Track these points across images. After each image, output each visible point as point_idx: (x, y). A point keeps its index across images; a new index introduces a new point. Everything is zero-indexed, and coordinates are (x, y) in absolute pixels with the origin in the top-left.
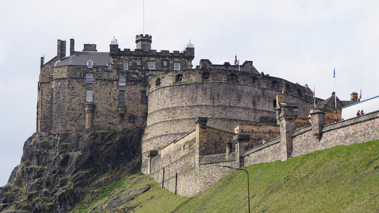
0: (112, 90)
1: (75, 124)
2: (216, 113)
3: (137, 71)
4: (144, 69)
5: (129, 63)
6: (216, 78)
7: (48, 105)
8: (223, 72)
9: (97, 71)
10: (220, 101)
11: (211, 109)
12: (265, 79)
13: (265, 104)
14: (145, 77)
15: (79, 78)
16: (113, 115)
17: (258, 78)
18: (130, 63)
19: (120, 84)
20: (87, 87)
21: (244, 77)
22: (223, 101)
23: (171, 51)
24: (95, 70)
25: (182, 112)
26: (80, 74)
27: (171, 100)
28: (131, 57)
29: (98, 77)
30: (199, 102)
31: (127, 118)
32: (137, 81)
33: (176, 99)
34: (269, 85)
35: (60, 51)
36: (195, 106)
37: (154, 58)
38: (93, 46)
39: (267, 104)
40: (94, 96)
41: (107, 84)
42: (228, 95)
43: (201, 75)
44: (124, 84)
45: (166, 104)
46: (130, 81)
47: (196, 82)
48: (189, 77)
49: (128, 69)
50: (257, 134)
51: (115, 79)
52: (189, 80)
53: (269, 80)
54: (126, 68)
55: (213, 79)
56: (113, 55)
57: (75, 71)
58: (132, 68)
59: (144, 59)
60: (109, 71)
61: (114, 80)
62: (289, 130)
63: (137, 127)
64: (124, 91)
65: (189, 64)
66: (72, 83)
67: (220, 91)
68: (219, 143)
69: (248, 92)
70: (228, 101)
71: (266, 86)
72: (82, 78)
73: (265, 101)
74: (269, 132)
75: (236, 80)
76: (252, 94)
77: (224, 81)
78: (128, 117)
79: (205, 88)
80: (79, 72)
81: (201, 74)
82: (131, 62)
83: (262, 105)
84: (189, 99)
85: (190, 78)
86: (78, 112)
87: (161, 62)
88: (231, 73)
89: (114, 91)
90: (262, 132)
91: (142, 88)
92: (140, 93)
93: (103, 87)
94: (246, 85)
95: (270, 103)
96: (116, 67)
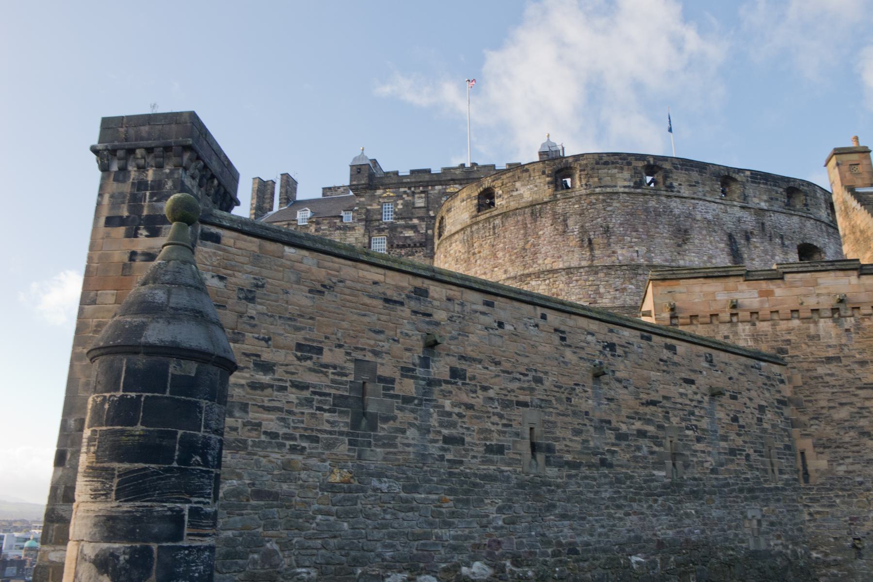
2: (602, 290)
3: (415, 221)
6: (596, 179)
9: (316, 230)
10: (614, 252)
13: (773, 256)
17: (739, 179)
21: (689, 175)
22: (624, 251)
28: (402, 190)
30: (546, 262)
32: (415, 246)
33: (478, 262)
34: (777, 199)
35: (255, 201)
36: (533, 277)
37: (457, 186)
38: (342, 189)
42: (641, 230)
43: (548, 179)
46: (398, 246)
47: (532, 201)
48: (513, 191)
52: (511, 199)
53: (775, 186)
55: (586, 185)
56: (357, 189)
58: (404, 215)
60: (346, 228)
67: (614, 221)
68: (409, 387)
69: (709, 221)
70: (643, 250)
74: (835, 310)
75: (664, 183)
76: (725, 228)
77: (625, 187)
79: (564, 215)
81: (548, 176)
82: (400, 202)
83: (761, 261)
84: (513, 257)
85: (515, 193)
88: (646, 163)
90: (792, 311)
95: (786, 254)
96: (364, 217)
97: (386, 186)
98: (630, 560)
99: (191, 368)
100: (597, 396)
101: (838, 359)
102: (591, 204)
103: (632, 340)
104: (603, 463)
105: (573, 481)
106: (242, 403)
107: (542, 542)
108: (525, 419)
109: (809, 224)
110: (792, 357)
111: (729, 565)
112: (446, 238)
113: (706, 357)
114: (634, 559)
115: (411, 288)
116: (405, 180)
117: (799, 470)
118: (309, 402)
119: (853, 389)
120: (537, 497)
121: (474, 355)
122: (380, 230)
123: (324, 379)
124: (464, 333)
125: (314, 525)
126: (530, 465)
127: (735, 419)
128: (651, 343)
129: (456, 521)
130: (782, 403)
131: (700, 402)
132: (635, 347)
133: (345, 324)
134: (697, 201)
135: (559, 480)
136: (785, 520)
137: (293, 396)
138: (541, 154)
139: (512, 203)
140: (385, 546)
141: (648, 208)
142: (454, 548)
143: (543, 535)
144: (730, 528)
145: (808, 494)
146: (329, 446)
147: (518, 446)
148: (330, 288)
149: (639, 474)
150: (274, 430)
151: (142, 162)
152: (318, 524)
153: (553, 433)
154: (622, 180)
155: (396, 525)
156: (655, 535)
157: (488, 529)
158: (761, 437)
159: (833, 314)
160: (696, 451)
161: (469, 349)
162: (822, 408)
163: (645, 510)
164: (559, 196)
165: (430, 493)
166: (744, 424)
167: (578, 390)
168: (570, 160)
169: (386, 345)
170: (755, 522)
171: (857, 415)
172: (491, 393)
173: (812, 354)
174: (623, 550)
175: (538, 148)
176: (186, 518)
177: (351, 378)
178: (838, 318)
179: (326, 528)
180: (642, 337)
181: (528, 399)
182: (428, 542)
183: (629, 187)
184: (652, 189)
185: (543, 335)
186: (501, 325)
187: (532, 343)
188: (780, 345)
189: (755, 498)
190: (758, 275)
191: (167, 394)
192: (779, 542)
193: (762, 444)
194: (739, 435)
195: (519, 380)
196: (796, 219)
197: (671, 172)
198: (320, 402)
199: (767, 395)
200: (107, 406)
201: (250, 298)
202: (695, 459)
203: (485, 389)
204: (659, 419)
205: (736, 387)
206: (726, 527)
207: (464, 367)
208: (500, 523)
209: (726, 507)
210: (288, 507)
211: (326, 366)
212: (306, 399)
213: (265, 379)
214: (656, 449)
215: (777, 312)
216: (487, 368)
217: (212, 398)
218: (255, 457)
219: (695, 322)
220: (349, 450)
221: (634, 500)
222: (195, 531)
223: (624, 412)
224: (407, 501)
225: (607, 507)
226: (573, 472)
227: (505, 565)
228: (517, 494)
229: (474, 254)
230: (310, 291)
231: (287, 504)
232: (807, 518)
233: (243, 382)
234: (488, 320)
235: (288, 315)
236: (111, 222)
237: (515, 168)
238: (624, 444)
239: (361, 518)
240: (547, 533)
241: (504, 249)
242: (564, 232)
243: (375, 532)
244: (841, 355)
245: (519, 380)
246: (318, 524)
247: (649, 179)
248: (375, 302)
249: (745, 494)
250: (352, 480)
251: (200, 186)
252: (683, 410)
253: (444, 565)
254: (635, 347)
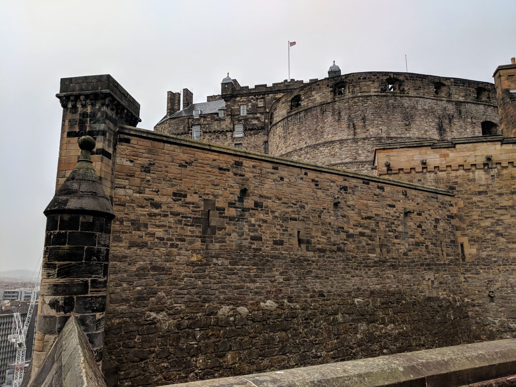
2: (360, 152)
3: (259, 115)
5: (248, 106)
6: (358, 88)
8: (371, 78)
10: (368, 130)
11: (351, 147)
12: (459, 86)
15: (182, 134)
19: (236, 136)
22: (374, 130)
23: (306, 81)
25: (300, 158)
26: (184, 127)
27: (285, 142)
28: (251, 97)
30: (328, 137)
32: (259, 129)
33: (291, 138)
35: (169, 105)
37: (281, 94)
39: (468, 130)
41: (218, 137)
42: (384, 117)
43: (331, 89)
44: (241, 135)
46: (249, 130)
48: (310, 97)
49: (247, 114)
50: (441, 174)
51: (228, 129)
54: (243, 112)
55: (352, 92)
57: (178, 124)
58: (253, 112)
60: (220, 120)
61: (227, 131)
64: (241, 144)
68: (232, 212)
71: (462, 97)
72: (186, 133)
73: (463, 124)
74: (485, 165)
75: (399, 89)
76: (436, 114)
77: (375, 92)
80: (182, 126)
82: (250, 104)
84: (310, 135)
85: (311, 98)
88: (388, 77)
90: (459, 166)
91: (265, 138)
93: (213, 142)
94: (421, 96)
95: (474, 128)
96: (230, 113)
97: (242, 95)
98: (354, 301)
99: (91, 219)
100: (337, 216)
101: (486, 192)
102: (355, 103)
103: (357, 184)
104: (339, 249)
105: (322, 259)
106: (145, 224)
107: (305, 290)
108: (294, 227)
109: (490, 109)
110: (458, 191)
111: (414, 304)
112: (274, 125)
113: (403, 193)
114: (356, 300)
115: (233, 162)
116: (252, 92)
117: (459, 254)
118: (180, 222)
119: (494, 209)
120: (301, 267)
121: (267, 195)
122: (239, 121)
123: (188, 210)
124: (262, 183)
125: (183, 283)
126: (298, 250)
127: (420, 226)
128: (370, 186)
129: (258, 279)
130: (451, 217)
131: (398, 217)
132: (359, 188)
133: (198, 182)
134: (419, 99)
135: (314, 258)
136: (449, 281)
137: (171, 219)
138: (329, 73)
139: (310, 104)
140: (220, 292)
141: (389, 104)
142: (256, 293)
143: (305, 287)
144: (414, 285)
145: (464, 267)
146: (191, 243)
147: (291, 241)
148: (190, 164)
149: (360, 256)
150: (162, 236)
151: (84, 102)
152: (185, 282)
153: (310, 234)
154: (373, 89)
155: (226, 282)
156: (369, 288)
157: (274, 284)
158: (436, 236)
159: (484, 167)
160: (395, 243)
161: (265, 192)
162: (474, 220)
163: (363, 275)
164: (336, 99)
165: (244, 265)
166: (426, 229)
167: (325, 211)
168: (343, 77)
169: (220, 192)
170: (430, 282)
171: (496, 224)
172: (277, 214)
173: (470, 189)
174: (350, 295)
175: (328, 69)
176: (89, 284)
177: (202, 208)
178: (487, 169)
179: (189, 284)
180: (364, 183)
181: (297, 216)
182: (242, 290)
183: (378, 92)
184: (391, 93)
185: (305, 183)
186: (282, 179)
187: (299, 187)
188: (451, 184)
189: (430, 269)
190: (440, 145)
191: (79, 231)
192: (445, 293)
193: (437, 240)
194: (422, 235)
195: (292, 207)
196: (482, 107)
197: (404, 82)
198: (185, 221)
199: (441, 212)
200: (52, 237)
201: (147, 169)
202: (394, 248)
203: (273, 212)
204: (373, 225)
205: (421, 208)
206: (412, 284)
207: (262, 201)
208: (281, 280)
209: (412, 274)
210: (170, 274)
211: (189, 203)
212: (178, 220)
213: (156, 211)
214: (370, 242)
215: (450, 166)
216: (274, 202)
217: (101, 231)
218: (152, 250)
219: (401, 172)
220: (201, 245)
221: (357, 269)
222: (94, 290)
223: (352, 222)
224: (231, 270)
225: (341, 273)
226: (322, 254)
227: (284, 302)
228: (291, 266)
229: (289, 133)
230: (179, 166)
231: (169, 273)
232: (463, 280)
233: (145, 213)
234: (275, 176)
235: (168, 179)
236: (70, 134)
237: (314, 83)
238: (351, 240)
239: (208, 279)
240: (307, 286)
241: (305, 130)
242: (339, 119)
243: (215, 285)
244: (488, 190)
245: (292, 207)
246: (185, 282)
247: (390, 86)
248: (214, 170)
249: (424, 267)
250: (203, 260)
251: (117, 113)
252: (387, 222)
253: (251, 302)
254: (359, 188)
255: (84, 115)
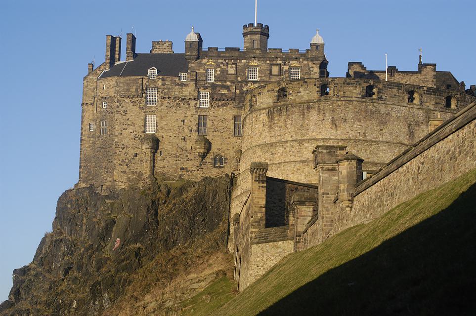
0: (186, 115)
1: (127, 171)
3: (228, 83)
4: (240, 80)
5: (216, 71)
6: (342, 93)
7: (92, 139)
12: (431, 94)
14: (241, 93)
16: (187, 156)
18: (217, 71)
20: (147, 110)
24: (160, 83)
26: (137, 89)
28: (220, 61)
29: (165, 95)
31: (210, 161)
35: (109, 53)
37: (256, 61)
40: (158, 124)
43: (318, 89)
45: (262, 137)
49: (215, 80)
51: (191, 97)
57: (128, 84)
58: (221, 78)
59: (239, 64)
60: (182, 85)
62: (327, 190)
63: (227, 175)
65: (315, 71)
66: (123, 104)
77: (356, 98)
78: (211, 159)
80: (134, 87)
82: (218, 69)
85: (299, 94)
86: (132, 152)
87: (269, 68)
89: (190, 116)
92: (233, 119)
93: (172, 110)
97: (209, 57)
102: (338, 106)
116: (222, 55)
122: (206, 88)
183: (359, 98)
242: (324, 119)
255: (260, 175)
